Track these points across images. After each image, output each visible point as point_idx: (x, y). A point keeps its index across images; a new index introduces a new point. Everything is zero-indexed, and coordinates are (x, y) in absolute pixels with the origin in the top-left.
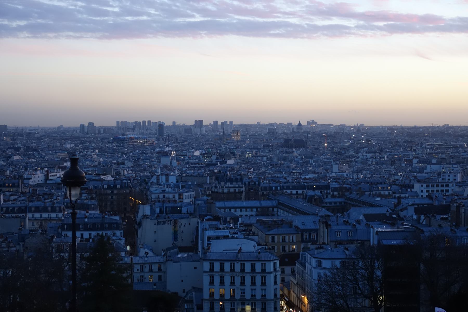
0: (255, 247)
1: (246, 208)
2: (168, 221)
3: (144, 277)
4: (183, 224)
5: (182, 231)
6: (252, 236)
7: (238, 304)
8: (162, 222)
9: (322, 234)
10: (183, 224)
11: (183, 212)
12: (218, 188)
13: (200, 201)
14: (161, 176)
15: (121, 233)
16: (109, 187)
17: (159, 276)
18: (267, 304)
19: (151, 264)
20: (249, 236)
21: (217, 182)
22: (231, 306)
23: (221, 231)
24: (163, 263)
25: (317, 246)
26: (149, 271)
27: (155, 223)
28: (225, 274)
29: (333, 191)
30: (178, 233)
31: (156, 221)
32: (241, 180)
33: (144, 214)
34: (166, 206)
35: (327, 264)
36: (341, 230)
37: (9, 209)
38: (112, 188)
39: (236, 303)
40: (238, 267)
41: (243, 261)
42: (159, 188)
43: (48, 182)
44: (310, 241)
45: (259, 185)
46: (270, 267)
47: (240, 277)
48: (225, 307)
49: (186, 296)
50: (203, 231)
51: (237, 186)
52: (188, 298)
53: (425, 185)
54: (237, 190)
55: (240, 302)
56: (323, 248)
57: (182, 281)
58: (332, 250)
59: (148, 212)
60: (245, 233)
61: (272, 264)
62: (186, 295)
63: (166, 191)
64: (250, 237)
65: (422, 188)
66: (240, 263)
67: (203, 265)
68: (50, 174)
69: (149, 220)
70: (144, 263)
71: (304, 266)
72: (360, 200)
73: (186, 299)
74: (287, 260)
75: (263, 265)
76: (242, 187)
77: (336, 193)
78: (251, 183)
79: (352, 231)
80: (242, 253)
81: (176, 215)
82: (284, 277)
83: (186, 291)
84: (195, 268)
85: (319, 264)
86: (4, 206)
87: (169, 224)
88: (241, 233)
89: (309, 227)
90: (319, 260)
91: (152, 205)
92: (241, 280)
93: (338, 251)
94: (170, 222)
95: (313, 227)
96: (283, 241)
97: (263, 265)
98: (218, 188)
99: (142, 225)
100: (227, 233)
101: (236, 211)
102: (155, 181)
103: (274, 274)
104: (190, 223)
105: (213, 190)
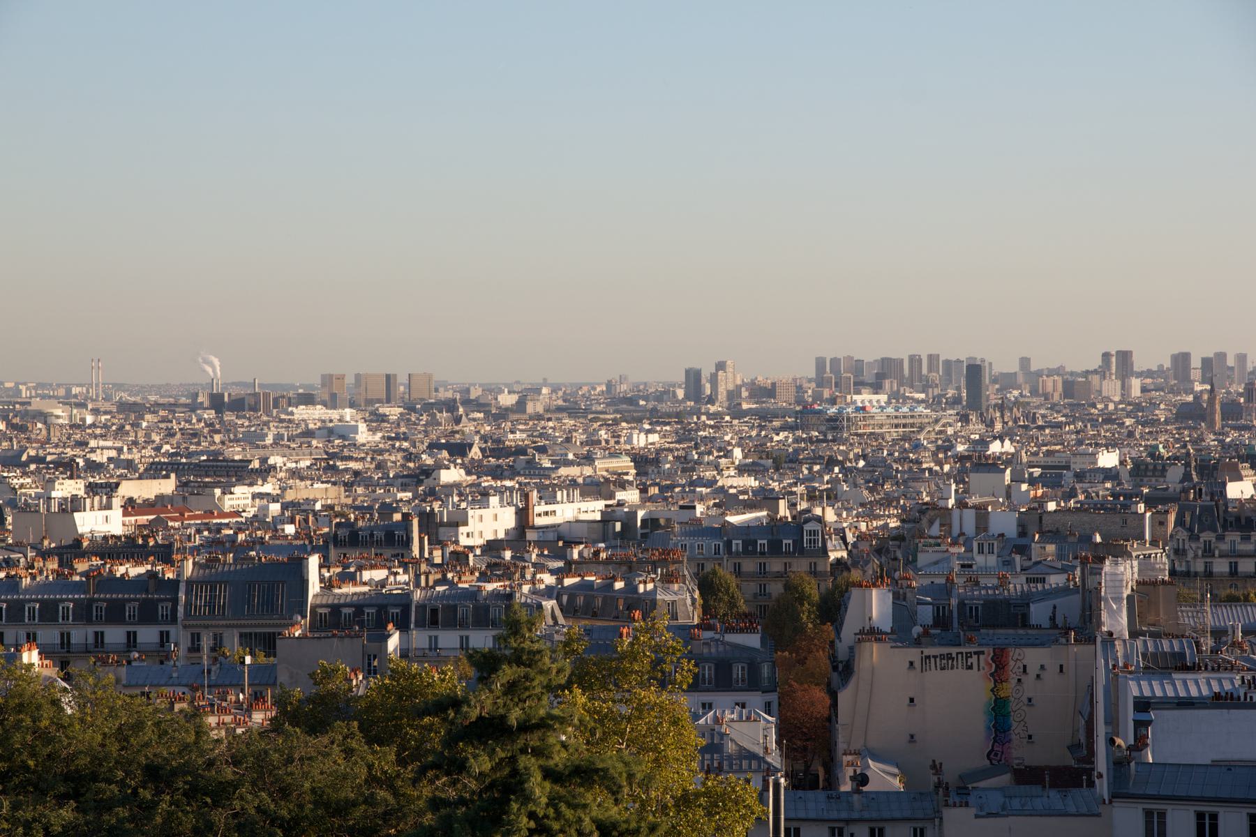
2: (969, 655)
4: (1033, 670)
8: (942, 657)
10: (1033, 670)
11: (1033, 621)
12: (1190, 555)
16: (750, 548)
19: (877, 825)
21: (1183, 535)
27: (911, 663)
30: (1013, 706)
31: (914, 654)
33: (867, 628)
37: (340, 612)
70: (848, 821)
87: (970, 667)
94: (974, 660)
98: (1189, 559)
99: (855, 669)
104: (1061, 666)
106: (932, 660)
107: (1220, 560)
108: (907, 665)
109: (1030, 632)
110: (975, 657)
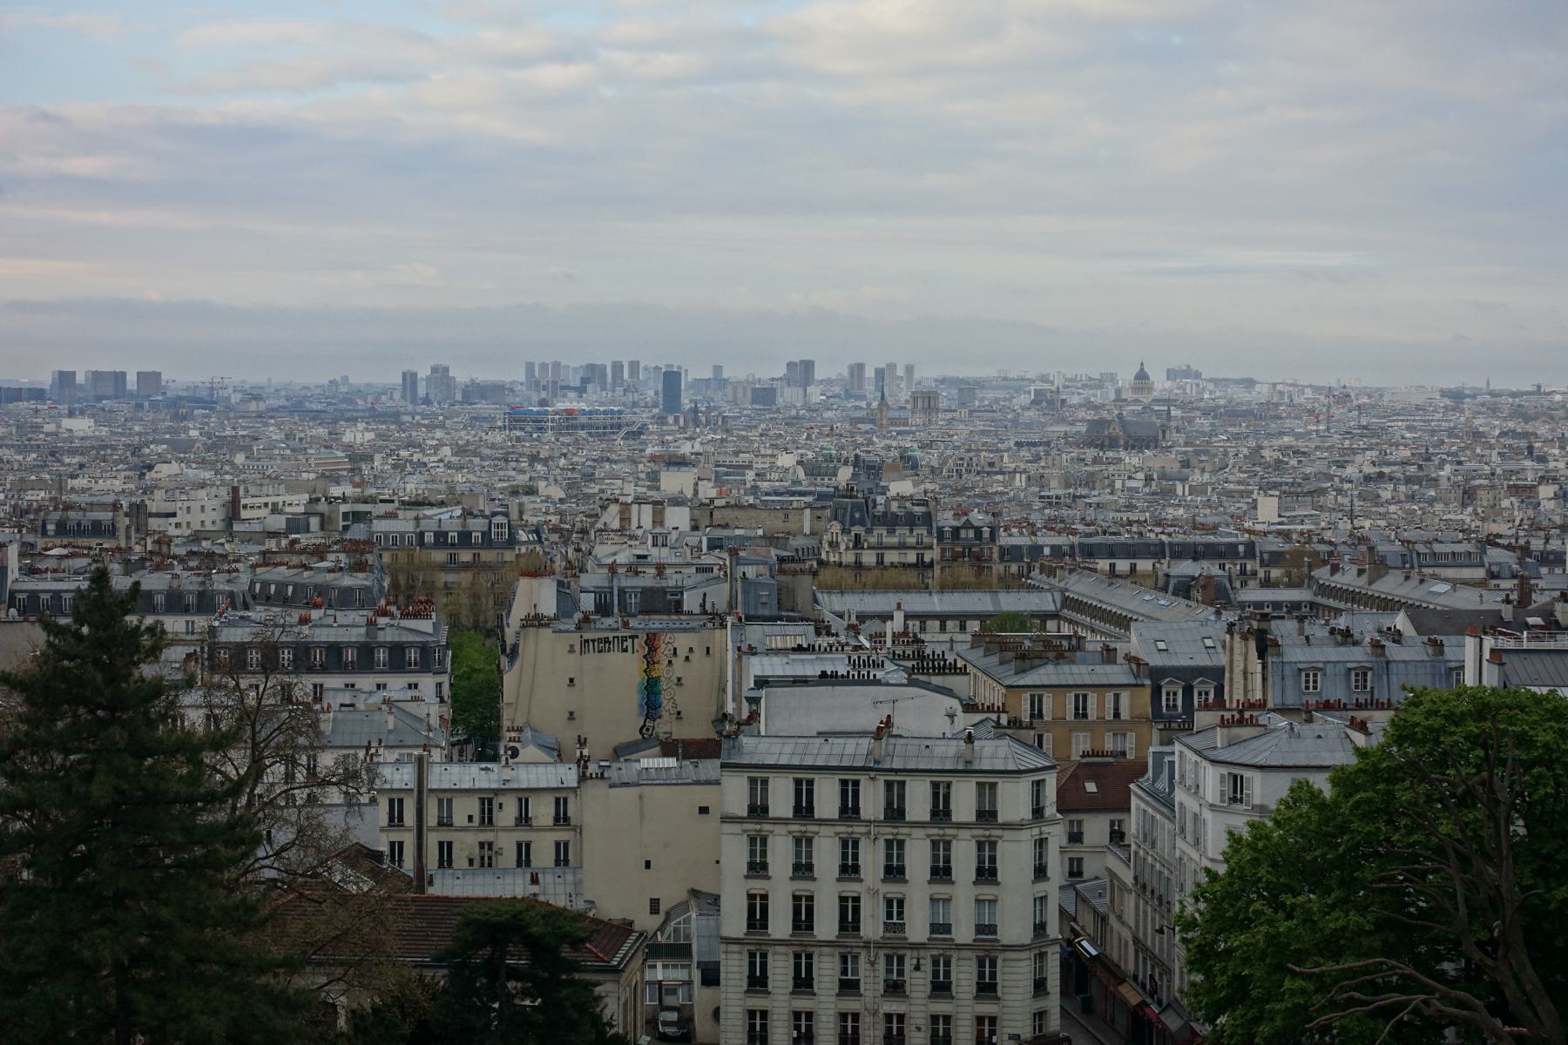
0: (951, 716)
1: (943, 618)
2: (624, 639)
3: (495, 849)
4: (682, 653)
5: (679, 679)
6: (946, 674)
7: (872, 964)
8: (600, 640)
10: (682, 653)
12: (843, 547)
13: (755, 567)
14: (635, 507)
15: (439, 685)
16: (442, 540)
17: (558, 844)
18: (999, 963)
19: (523, 795)
20: (928, 674)
22: (844, 972)
23: (814, 657)
24: (574, 790)
25: (1227, 715)
26: (517, 825)
27: (572, 646)
28: (814, 828)
29: (1267, 566)
30: (664, 685)
31: (575, 639)
32: (927, 519)
34: (624, 584)
35: (1267, 791)
36: (1320, 665)
37: (39, 597)
38: (453, 545)
39: (862, 959)
40: (872, 801)
41: (896, 771)
42: (625, 546)
43: (237, 527)
45: (993, 537)
46: (1014, 801)
47: (881, 844)
48: (815, 975)
49: (662, 928)
51: (912, 540)
52: (669, 938)
55: (882, 953)
56: (1252, 723)
57: (648, 865)
58: (1292, 729)
59: (548, 605)
61: (1023, 788)
62: (665, 924)
63: (649, 558)
64: (937, 680)
66: (882, 779)
68: (243, 501)
69: (548, 631)
70: (497, 792)
71: (1167, 802)
72: (1370, 593)
74: (1091, 787)
75: (987, 791)
76: (931, 548)
77: (1276, 573)
78: (963, 534)
79: (1371, 669)
80: (892, 741)
81: (657, 617)
82: (1080, 860)
83: (663, 907)
84: (704, 810)
85: (1235, 791)
86: (18, 587)
87: (625, 650)
88: (897, 665)
89: (1184, 662)
90: (1236, 771)
91: (566, 580)
92: (889, 857)
93: (1319, 737)
94: (629, 643)
95: (1203, 660)
96: (1077, 715)
97: (987, 791)
102: (616, 525)
103: (1036, 831)
104: (708, 649)
105: (824, 556)
106: (591, 643)
107: (868, 551)
108: (568, 648)
109: (683, 617)
110: (630, 641)
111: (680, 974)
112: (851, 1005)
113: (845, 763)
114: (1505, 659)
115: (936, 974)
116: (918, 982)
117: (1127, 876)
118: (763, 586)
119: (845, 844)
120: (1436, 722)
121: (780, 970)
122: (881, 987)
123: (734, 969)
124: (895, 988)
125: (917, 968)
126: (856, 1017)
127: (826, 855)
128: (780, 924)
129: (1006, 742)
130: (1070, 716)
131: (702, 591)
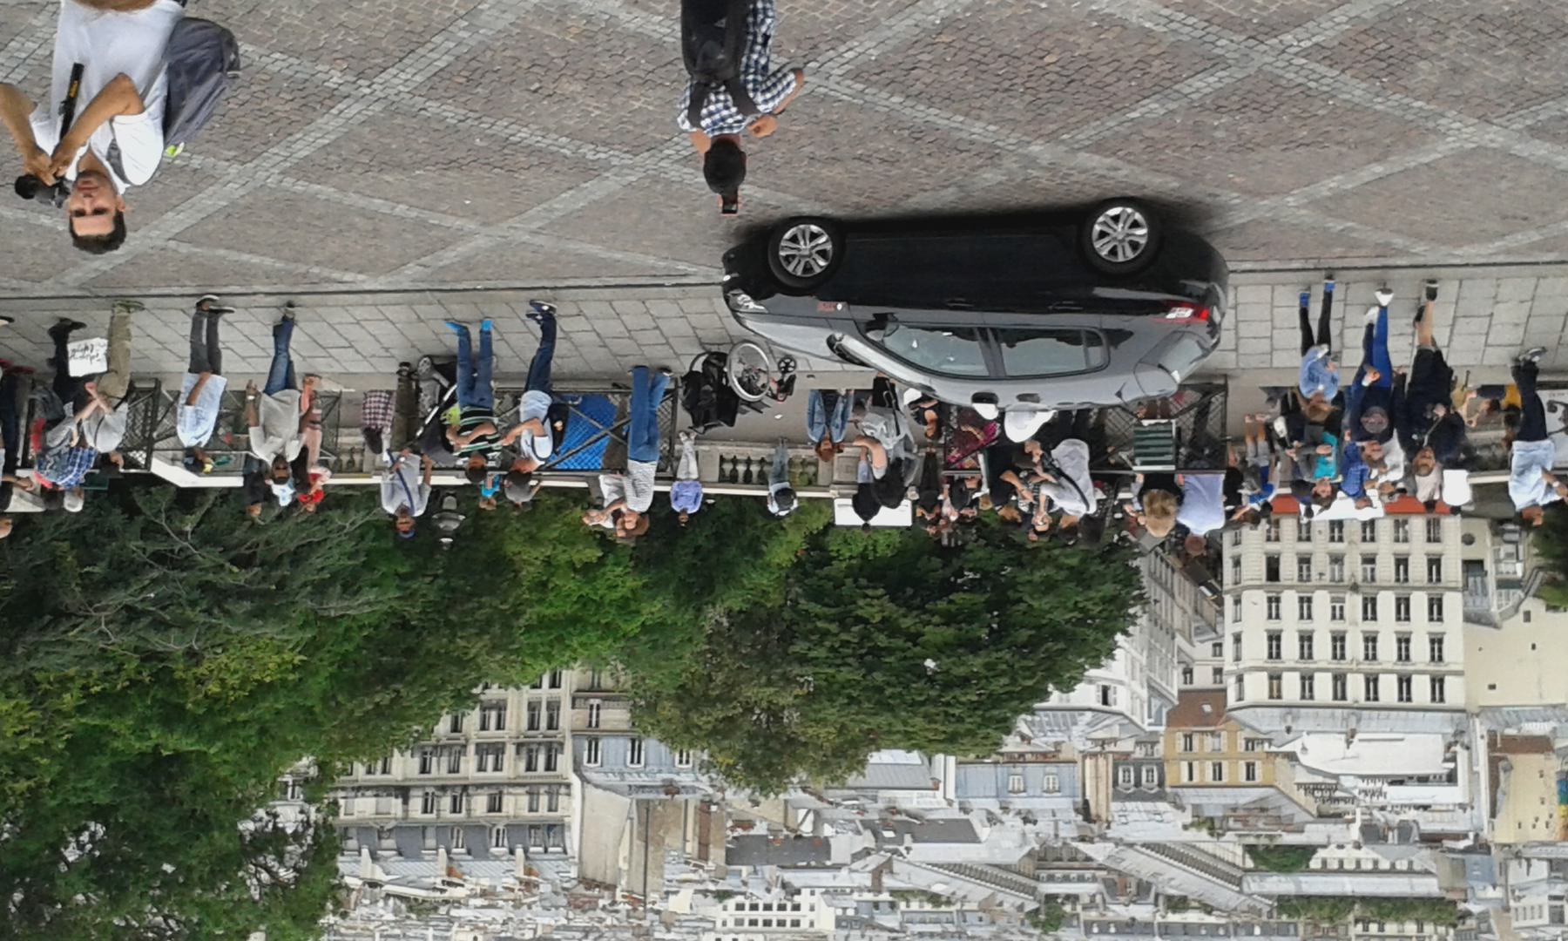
0: (1304, 749)
1: (1341, 870)
4: (1541, 824)
9: (1102, 787)
10: (1541, 824)
11: (1545, 864)
22: (1373, 570)
30: (1556, 799)
35: (1085, 694)
40: (1356, 687)
44: (1138, 765)
46: (1256, 687)
50: (1472, 800)
53: (804, 925)
54: (1373, 928)
57: (1534, 647)
60: (1338, 794)
61: (1249, 698)
64: (1319, 779)
65: (812, 916)
66: (1349, 701)
67: (1468, 697)
73: (1520, 593)
74: (1207, 708)
75: (1275, 692)
83: (1521, 616)
84: (1492, 687)
90: (1105, 708)
92: (1343, 648)
95: (1130, 805)
97: (1275, 692)
100: (1396, 794)
101: (1376, 862)
111: (1503, 567)
112: (1368, 548)
113: (1375, 713)
114: (930, 784)
115: (1309, 569)
116: (1320, 563)
117: (1179, 640)
118: (1477, 878)
119: (1374, 657)
120: (982, 732)
121: (1418, 569)
122: (1346, 560)
123: (1452, 570)
124: (1337, 559)
125: (1321, 574)
126: (1364, 539)
127: (1387, 650)
128: (1419, 602)
129: (1264, 728)
130: (1225, 765)
131: (1530, 879)
